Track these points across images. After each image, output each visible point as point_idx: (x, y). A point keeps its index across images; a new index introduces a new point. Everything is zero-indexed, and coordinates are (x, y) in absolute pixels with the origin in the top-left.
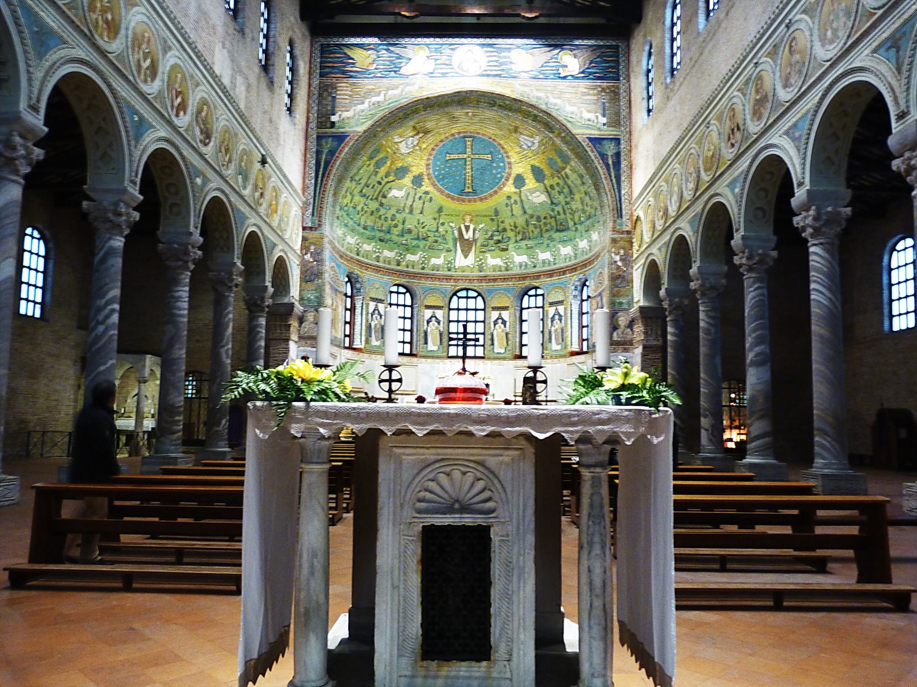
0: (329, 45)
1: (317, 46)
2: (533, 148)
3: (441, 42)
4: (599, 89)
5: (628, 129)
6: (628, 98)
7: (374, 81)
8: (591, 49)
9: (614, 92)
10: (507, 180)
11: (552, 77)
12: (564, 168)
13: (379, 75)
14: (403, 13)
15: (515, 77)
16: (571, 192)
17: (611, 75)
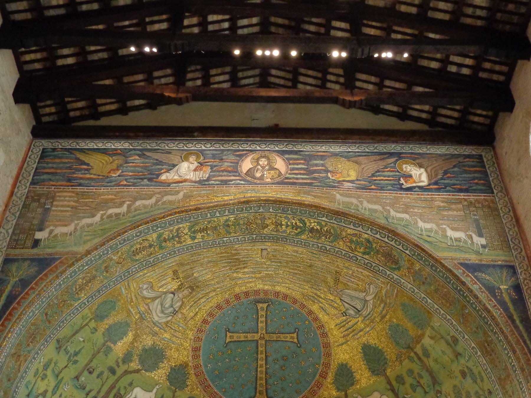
0: (54, 150)
1: (37, 151)
2: (364, 313)
3: (222, 148)
4: (466, 203)
5: (523, 253)
6: (511, 213)
7: (118, 189)
8: (443, 158)
9: (489, 207)
10: (324, 376)
11: (390, 187)
12: (419, 339)
13: (125, 183)
14: (167, 94)
15: (335, 187)
16: (435, 381)
17: (480, 187)
